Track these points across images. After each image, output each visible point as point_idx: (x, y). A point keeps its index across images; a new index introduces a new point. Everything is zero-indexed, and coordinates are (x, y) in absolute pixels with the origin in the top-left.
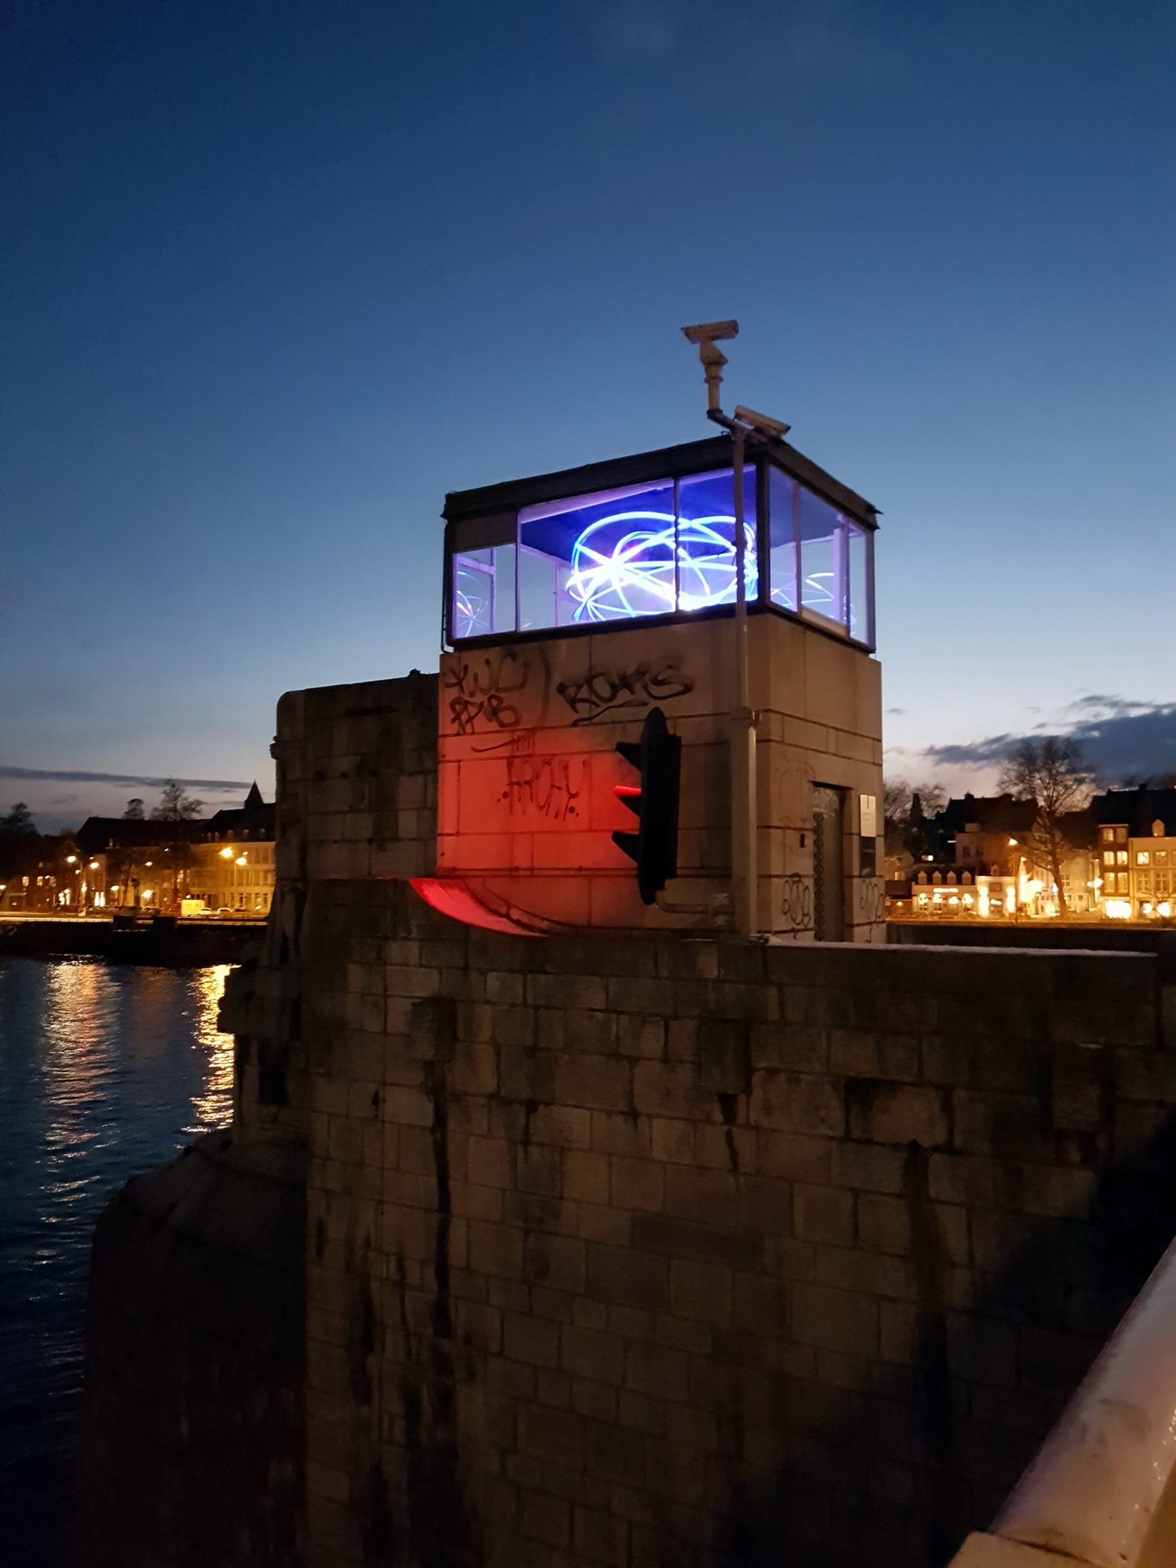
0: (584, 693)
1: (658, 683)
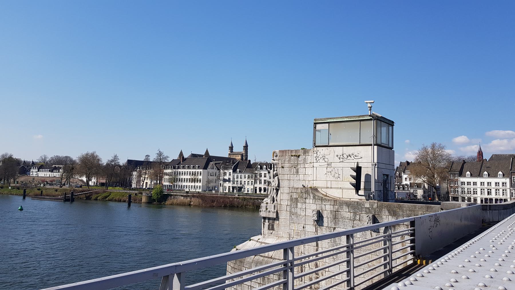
0: (342, 157)
1: (356, 156)
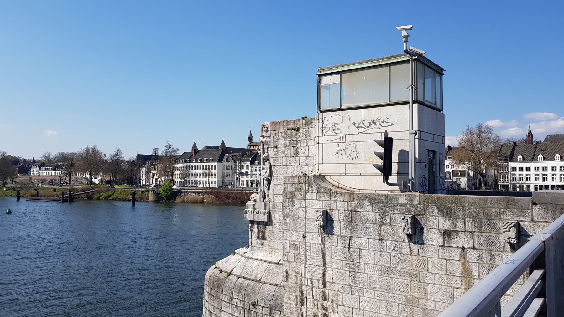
0: (361, 125)
1: (383, 122)
